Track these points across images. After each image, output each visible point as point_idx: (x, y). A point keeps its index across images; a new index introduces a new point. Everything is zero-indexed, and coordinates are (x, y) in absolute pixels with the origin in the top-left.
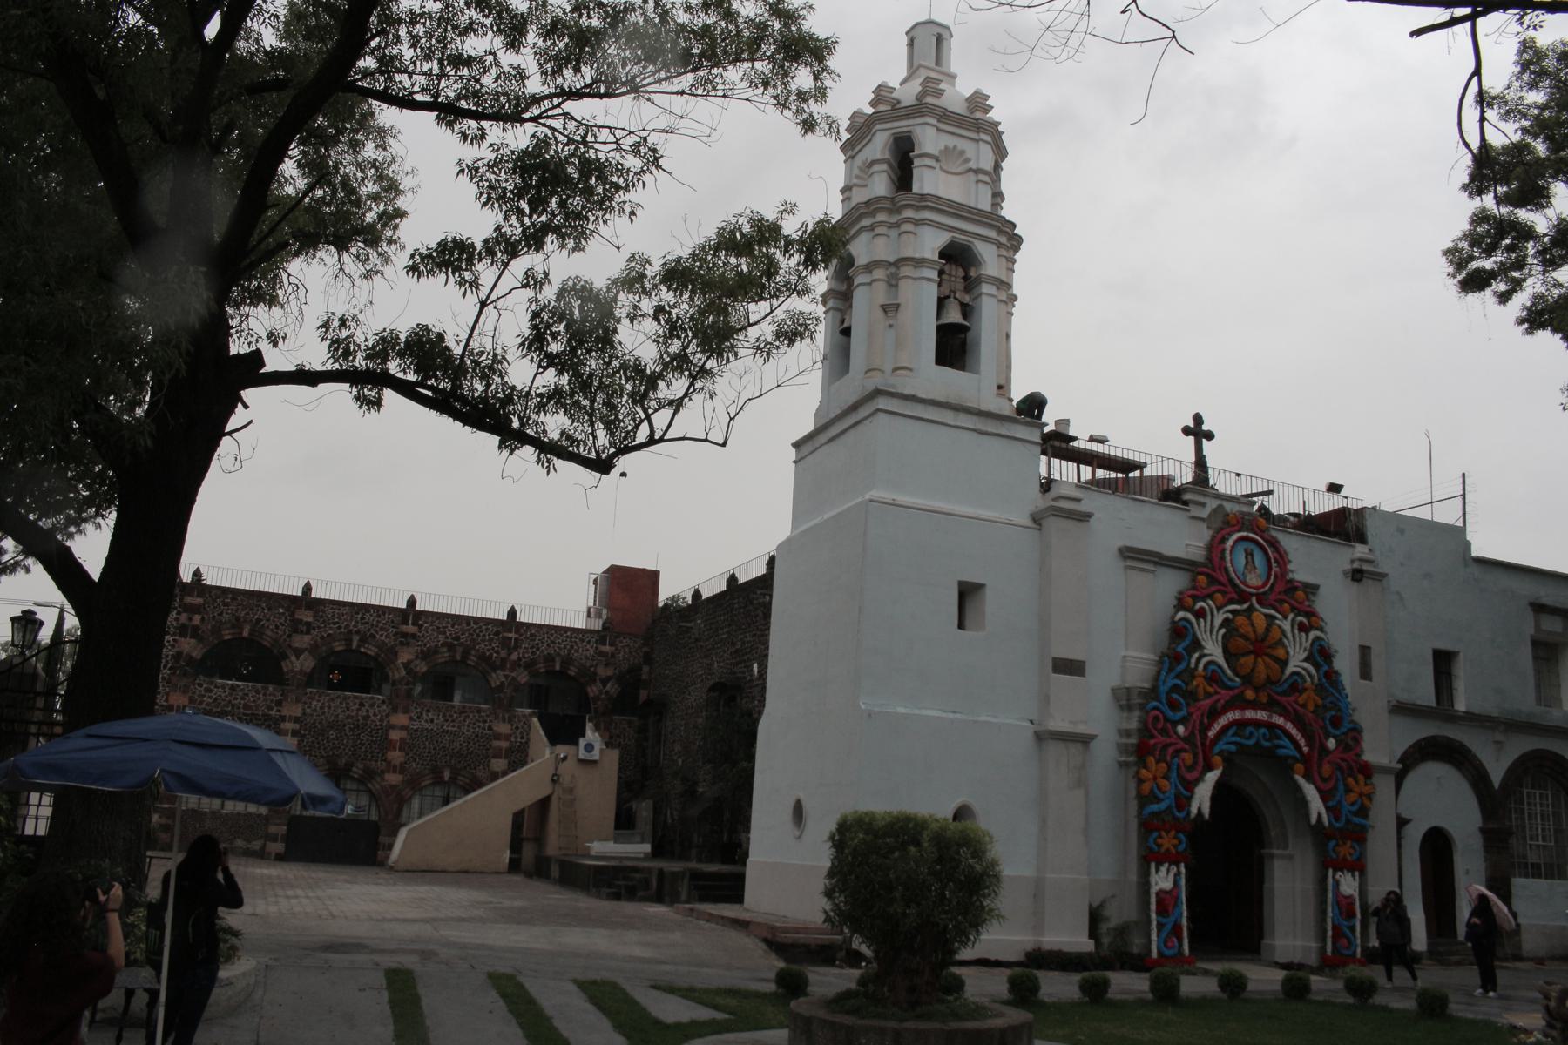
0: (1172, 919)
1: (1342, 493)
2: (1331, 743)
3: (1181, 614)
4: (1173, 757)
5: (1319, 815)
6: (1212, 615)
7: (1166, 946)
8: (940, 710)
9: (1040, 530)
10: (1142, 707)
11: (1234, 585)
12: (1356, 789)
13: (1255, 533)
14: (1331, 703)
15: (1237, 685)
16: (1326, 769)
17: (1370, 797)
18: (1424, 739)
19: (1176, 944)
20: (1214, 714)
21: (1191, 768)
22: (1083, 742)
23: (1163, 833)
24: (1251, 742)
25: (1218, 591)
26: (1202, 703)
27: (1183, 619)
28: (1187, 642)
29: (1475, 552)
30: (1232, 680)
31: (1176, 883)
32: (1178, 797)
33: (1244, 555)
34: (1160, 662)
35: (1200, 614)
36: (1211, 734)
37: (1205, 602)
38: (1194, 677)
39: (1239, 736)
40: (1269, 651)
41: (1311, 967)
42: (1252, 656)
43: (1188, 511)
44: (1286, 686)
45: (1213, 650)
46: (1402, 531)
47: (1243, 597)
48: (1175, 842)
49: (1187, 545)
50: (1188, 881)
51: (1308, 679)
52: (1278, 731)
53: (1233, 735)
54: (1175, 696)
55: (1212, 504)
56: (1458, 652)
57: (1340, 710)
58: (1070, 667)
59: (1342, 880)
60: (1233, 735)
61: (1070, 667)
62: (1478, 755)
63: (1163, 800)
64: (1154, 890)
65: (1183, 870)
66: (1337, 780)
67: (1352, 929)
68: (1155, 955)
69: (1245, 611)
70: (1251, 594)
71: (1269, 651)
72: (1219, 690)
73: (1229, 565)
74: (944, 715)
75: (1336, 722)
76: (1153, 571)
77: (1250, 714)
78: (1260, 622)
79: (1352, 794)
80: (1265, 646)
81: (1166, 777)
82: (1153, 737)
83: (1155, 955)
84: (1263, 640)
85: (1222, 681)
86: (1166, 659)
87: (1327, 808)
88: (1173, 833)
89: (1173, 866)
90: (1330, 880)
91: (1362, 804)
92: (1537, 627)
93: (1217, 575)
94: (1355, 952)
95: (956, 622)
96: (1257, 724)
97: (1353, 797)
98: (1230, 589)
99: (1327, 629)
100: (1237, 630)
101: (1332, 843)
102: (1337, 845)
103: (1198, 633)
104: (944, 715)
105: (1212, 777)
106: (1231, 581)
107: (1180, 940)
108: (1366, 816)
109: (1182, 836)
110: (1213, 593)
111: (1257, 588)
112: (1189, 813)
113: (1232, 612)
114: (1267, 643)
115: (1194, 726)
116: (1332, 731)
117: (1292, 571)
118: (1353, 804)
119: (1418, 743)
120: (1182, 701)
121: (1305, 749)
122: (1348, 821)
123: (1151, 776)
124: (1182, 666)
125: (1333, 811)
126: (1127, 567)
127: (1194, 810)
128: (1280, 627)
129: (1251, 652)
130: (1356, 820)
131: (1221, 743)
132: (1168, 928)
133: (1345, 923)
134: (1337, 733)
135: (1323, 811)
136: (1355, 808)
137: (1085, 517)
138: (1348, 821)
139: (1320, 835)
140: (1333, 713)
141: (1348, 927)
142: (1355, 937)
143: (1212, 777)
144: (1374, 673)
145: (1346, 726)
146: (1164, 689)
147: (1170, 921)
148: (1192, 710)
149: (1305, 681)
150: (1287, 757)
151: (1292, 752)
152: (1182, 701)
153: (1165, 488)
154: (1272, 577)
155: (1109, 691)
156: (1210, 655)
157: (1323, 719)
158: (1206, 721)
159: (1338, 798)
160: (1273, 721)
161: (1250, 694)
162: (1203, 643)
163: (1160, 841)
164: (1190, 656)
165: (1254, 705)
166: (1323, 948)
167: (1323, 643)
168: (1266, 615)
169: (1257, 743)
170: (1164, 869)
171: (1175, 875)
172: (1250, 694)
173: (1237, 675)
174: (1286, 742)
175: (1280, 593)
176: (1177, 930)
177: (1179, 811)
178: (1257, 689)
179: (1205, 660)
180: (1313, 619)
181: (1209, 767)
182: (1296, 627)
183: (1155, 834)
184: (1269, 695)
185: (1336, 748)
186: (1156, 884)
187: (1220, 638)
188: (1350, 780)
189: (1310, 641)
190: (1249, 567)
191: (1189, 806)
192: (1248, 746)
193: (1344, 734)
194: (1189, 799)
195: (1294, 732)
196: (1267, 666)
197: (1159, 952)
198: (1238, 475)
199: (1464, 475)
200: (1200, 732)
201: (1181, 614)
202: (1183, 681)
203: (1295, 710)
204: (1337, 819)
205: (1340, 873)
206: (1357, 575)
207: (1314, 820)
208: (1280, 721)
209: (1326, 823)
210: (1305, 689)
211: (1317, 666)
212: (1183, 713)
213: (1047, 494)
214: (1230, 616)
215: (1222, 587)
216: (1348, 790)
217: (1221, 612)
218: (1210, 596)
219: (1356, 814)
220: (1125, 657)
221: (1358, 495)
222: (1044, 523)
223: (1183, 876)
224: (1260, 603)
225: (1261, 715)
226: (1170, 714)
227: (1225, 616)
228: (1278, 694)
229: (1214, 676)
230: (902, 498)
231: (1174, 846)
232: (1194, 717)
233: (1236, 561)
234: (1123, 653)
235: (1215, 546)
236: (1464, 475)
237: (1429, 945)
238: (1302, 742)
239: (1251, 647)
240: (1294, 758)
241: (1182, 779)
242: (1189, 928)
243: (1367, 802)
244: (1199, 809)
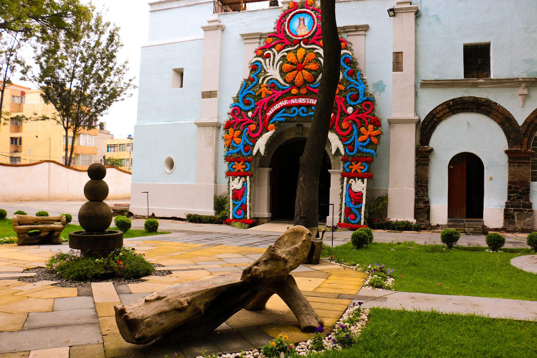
2: (350, 110)
5: (338, 150)
6: (274, 55)
7: (237, 214)
8: (164, 121)
14: (352, 87)
15: (285, 88)
17: (378, 136)
18: (453, 100)
19: (243, 213)
20: (271, 104)
21: (253, 132)
22: (212, 126)
23: (236, 163)
25: (279, 43)
26: (263, 100)
27: (256, 61)
30: (285, 86)
31: (243, 185)
32: (245, 146)
33: (299, 21)
34: (242, 84)
35: (268, 56)
36: (269, 114)
37: (271, 50)
38: (260, 88)
42: (296, 71)
45: (274, 73)
48: (244, 166)
57: (358, 90)
59: (353, 184)
60: (283, 113)
62: (502, 105)
63: (237, 148)
64: (231, 189)
66: (353, 130)
67: (359, 210)
68: (231, 218)
69: (294, 50)
70: (300, 40)
71: (305, 67)
73: (286, 29)
74: (164, 123)
75: (355, 98)
77: (293, 101)
78: (301, 53)
79: (363, 136)
83: (231, 218)
87: (344, 145)
88: (242, 162)
89: (243, 178)
90: (345, 183)
91: (371, 141)
94: (360, 222)
95: (179, 85)
96: (299, 106)
99: (352, 48)
100: (287, 59)
101: (348, 164)
102: (352, 165)
103: (265, 66)
104: (164, 123)
105: (266, 136)
107: (245, 212)
111: (303, 36)
112: (252, 154)
113: (287, 52)
114: (303, 64)
115: (258, 112)
116: (352, 103)
118: (365, 141)
119: (447, 103)
120: (252, 100)
122: (358, 151)
123: (231, 137)
124: (254, 83)
125: (350, 147)
126: (245, 44)
127: (255, 152)
128: (315, 53)
129: (295, 70)
131: (275, 117)
133: (354, 206)
134: (355, 103)
138: (358, 151)
139: (345, 160)
140: (353, 93)
141: (357, 209)
142: (361, 215)
143: (266, 136)
144: (404, 67)
146: (241, 97)
147: (239, 203)
152: (252, 100)
154: (314, 29)
156: (272, 75)
160: (310, 103)
161: (294, 91)
162: (267, 71)
164: (259, 78)
165: (297, 96)
166: (340, 219)
167: (348, 56)
168: (309, 49)
169: (298, 115)
170: (237, 179)
171: (243, 182)
172: (294, 91)
173: (287, 83)
175: (319, 35)
178: (299, 88)
181: (268, 131)
183: (232, 163)
184: (308, 90)
185: (353, 112)
187: (278, 66)
190: (300, 26)
191: (253, 150)
192: (294, 117)
193: (359, 104)
194: (254, 146)
200: (262, 114)
202: (253, 91)
204: (352, 150)
207: (333, 152)
209: (343, 152)
212: (253, 106)
214: (286, 54)
215: (282, 41)
216: (360, 134)
217: (280, 53)
218: (274, 46)
219: (367, 147)
224: (306, 44)
225: (301, 101)
226: (244, 107)
227: (282, 54)
228: (314, 88)
230: (154, 44)
232: (258, 107)
235: (280, 23)
237: (449, 221)
239: (295, 67)
241: (249, 136)
243: (374, 140)
244: (258, 151)
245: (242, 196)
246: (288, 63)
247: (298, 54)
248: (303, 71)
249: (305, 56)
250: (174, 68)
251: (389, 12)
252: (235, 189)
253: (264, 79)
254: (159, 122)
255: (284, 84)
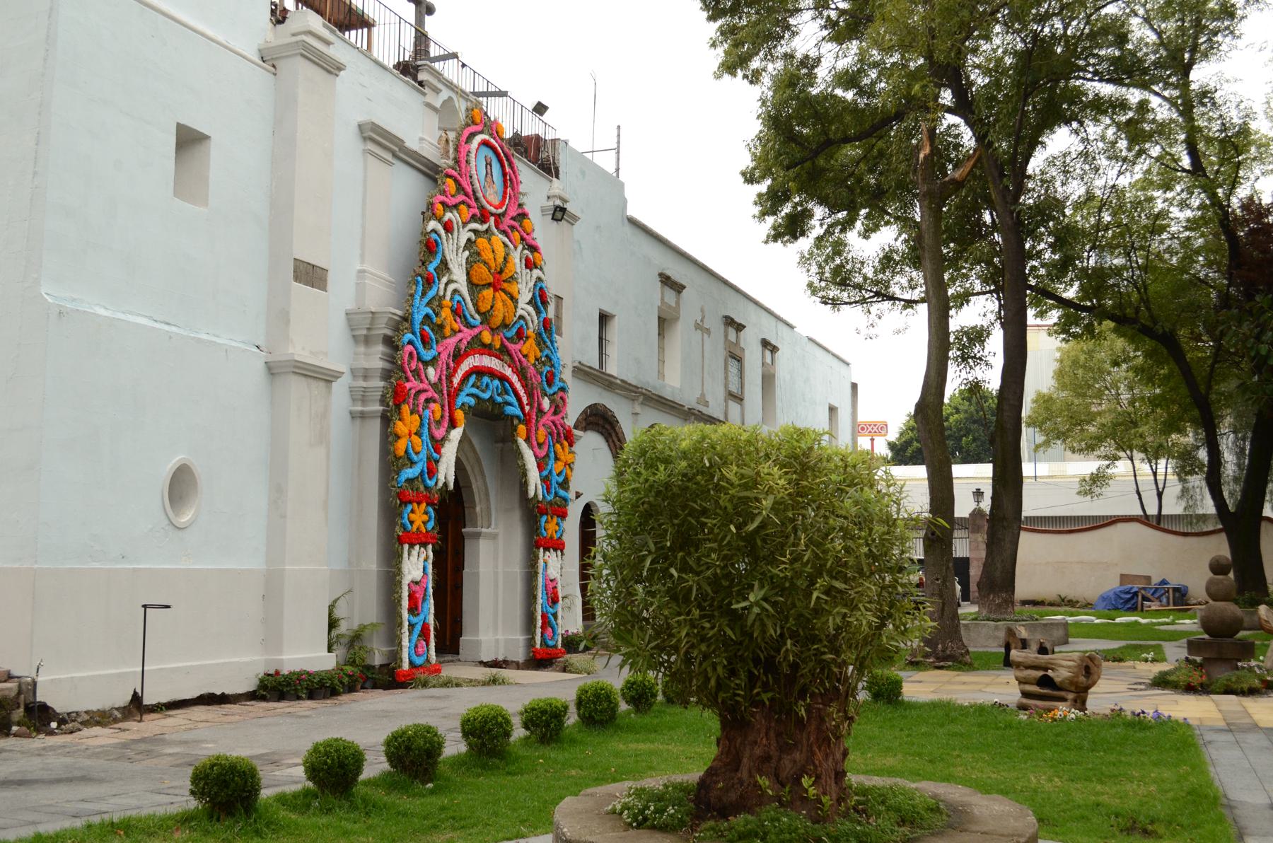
0: (422, 617)
1: (545, 118)
2: (546, 403)
3: (433, 224)
4: (425, 408)
8: (150, 318)
9: (275, 74)
10: (388, 341)
11: (477, 199)
12: (562, 457)
13: (494, 138)
16: (542, 432)
18: (590, 407)
20: (458, 357)
24: (486, 396)
25: (463, 202)
27: (434, 231)
28: (436, 263)
29: (632, 211)
36: (456, 381)
39: (478, 388)
40: (505, 285)
41: (517, 663)
42: (491, 290)
43: (424, 94)
44: (514, 330)
46: (583, 173)
47: (483, 217)
49: (421, 139)
50: (434, 567)
51: (531, 325)
52: (507, 385)
53: (473, 386)
54: (427, 328)
55: (445, 94)
56: (613, 316)
57: (552, 366)
58: (311, 275)
59: (550, 561)
60: (473, 386)
61: (311, 275)
64: (406, 581)
65: (431, 554)
68: (406, 666)
70: (493, 215)
71: (505, 285)
72: (463, 328)
73: (474, 172)
75: (550, 381)
76: (391, 164)
80: (500, 281)
81: (419, 434)
82: (408, 380)
83: (406, 666)
84: (501, 272)
85: (465, 316)
86: (419, 278)
88: (424, 505)
90: (541, 563)
92: (662, 299)
93: (464, 183)
96: (492, 373)
97: (560, 465)
98: (473, 203)
99: (545, 269)
100: (479, 254)
101: (544, 519)
103: (447, 252)
106: (474, 192)
108: (567, 489)
109: (430, 510)
110: (460, 203)
113: (475, 231)
114: (504, 276)
117: (524, 194)
119: (584, 412)
120: (433, 337)
121: (527, 408)
122: (556, 494)
123: (407, 431)
125: (546, 480)
129: (489, 285)
130: (562, 493)
132: (418, 628)
135: (539, 482)
136: (560, 479)
137: (333, 68)
138: (556, 494)
140: (548, 368)
145: (558, 384)
146: (418, 318)
148: (441, 349)
149: (528, 328)
150: (512, 417)
151: (518, 412)
152: (433, 337)
153: (401, 60)
155: (343, 316)
157: (541, 374)
158: (452, 365)
159: (549, 467)
161: (487, 337)
162: (451, 266)
163: (411, 515)
165: (487, 349)
166: (533, 638)
173: (478, 311)
174: (512, 399)
176: (425, 629)
177: (430, 478)
179: (452, 287)
180: (536, 254)
181: (453, 424)
182: (524, 262)
183: (409, 508)
186: (409, 573)
187: (464, 261)
188: (558, 446)
189: (534, 281)
195: (518, 386)
196: (505, 304)
197: (411, 663)
198: (464, 65)
199: (619, 127)
201: (433, 224)
202: (434, 311)
203: (520, 361)
204: (549, 492)
205: (547, 553)
206: (559, 213)
208: (508, 372)
209: (540, 497)
210: (527, 337)
211: (538, 312)
212: (433, 353)
213: (280, 27)
214: (472, 236)
218: (456, 206)
220: (362, 272)
221: (556, 126)
222: (279, 64)
223: (430, 561)
229: (458, 312)
231: (424, 523)
233: (479, 165)
234: (359, 268)
236: (619, 127)
238: (525, 400)
240: (518, 417)
242: (435, 629)
245: (424, 600)
246: (485, 263)
247: (495, 249)
248: (503, 294)
249: (505, 258)
250: (182, 122)
251: (555, 210)
252: (412, 582)
253: (447, 284)
254: (131, 313)
255: (473, 312)
